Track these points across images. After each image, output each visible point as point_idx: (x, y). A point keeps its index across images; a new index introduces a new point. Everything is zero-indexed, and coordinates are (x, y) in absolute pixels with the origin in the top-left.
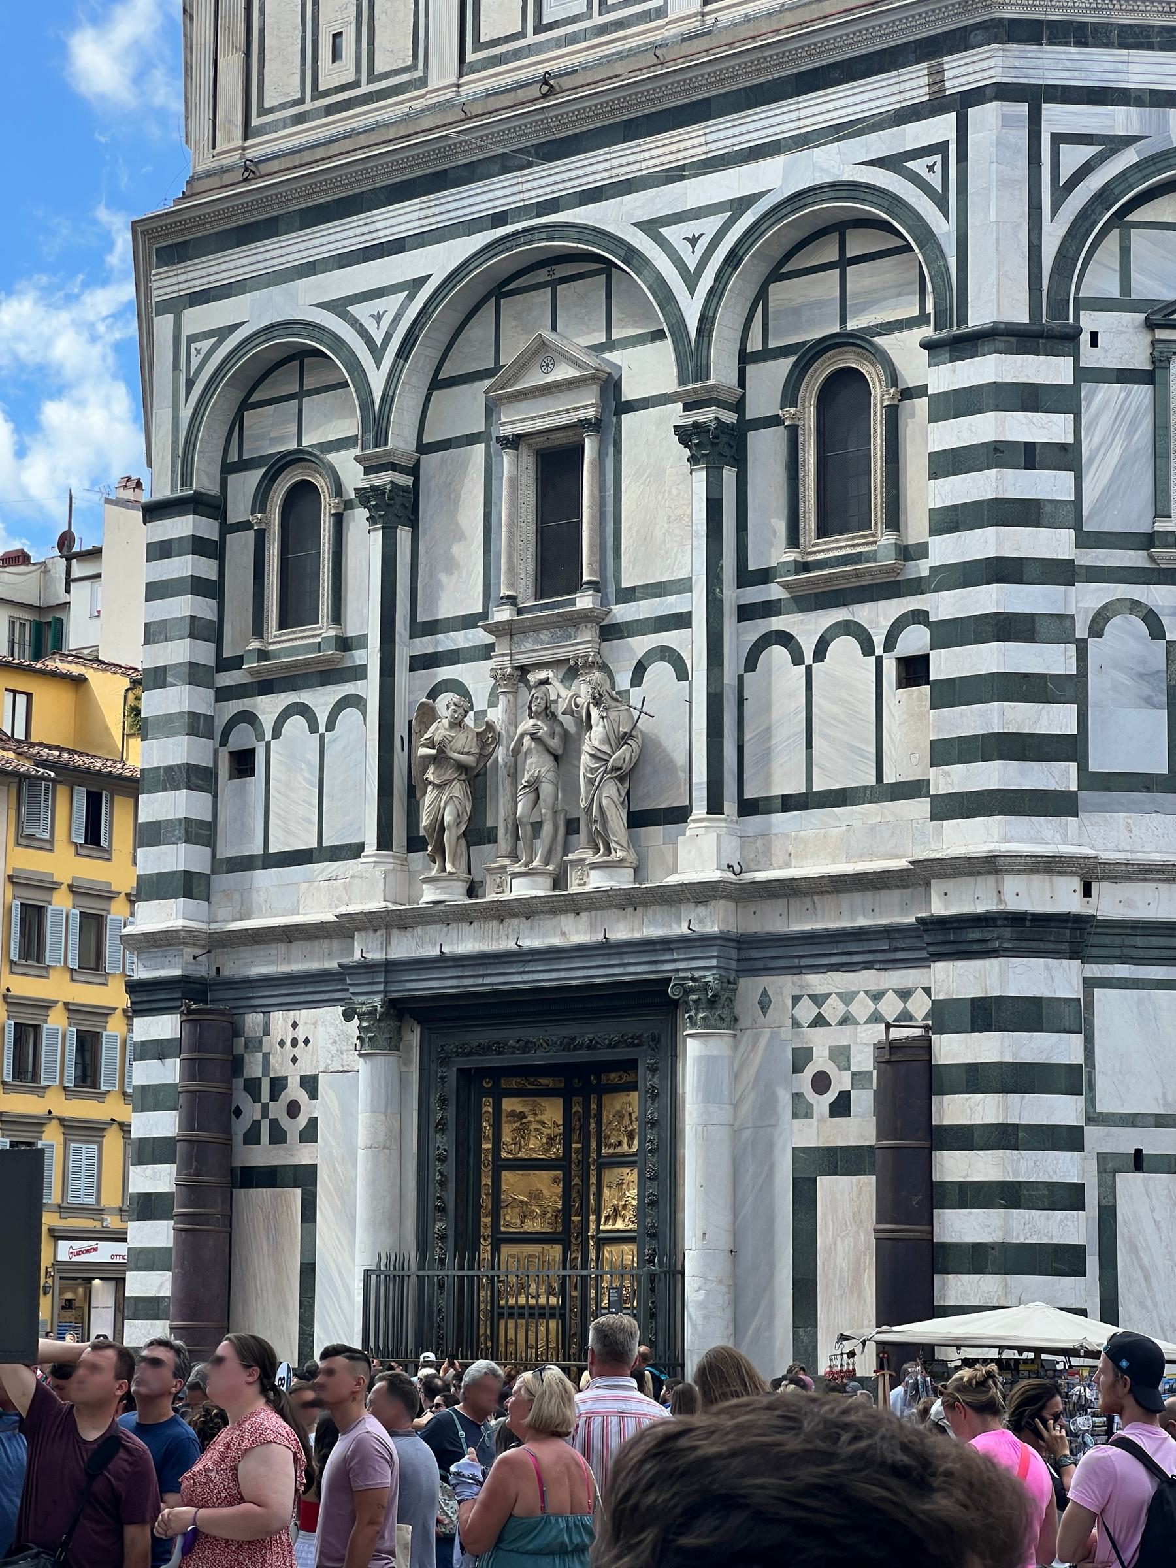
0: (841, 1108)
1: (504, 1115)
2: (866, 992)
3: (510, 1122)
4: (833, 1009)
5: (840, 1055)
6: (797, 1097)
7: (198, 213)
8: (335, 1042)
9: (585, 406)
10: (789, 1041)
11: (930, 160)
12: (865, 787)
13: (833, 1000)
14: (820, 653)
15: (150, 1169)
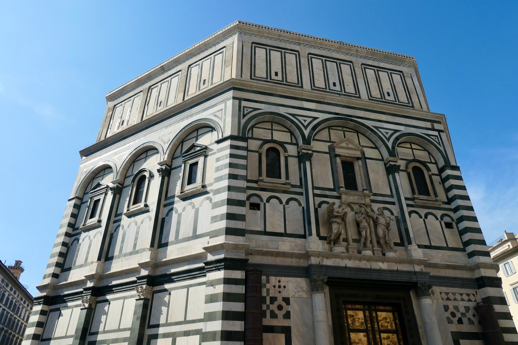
0: (460, 321)
1: (348, 316)
2: (458, 293)
3: (350, 318)
4: (451, 296)
5: (456, 308)
6: (448, 318)
7: (252, 84)
8: (296, 288)
9: (358, 154)
10: (442, 303)
11: (435, 137)
12: (444, 247)
13: (450, 294)
14: (426, 217)
15: (231, 322)
